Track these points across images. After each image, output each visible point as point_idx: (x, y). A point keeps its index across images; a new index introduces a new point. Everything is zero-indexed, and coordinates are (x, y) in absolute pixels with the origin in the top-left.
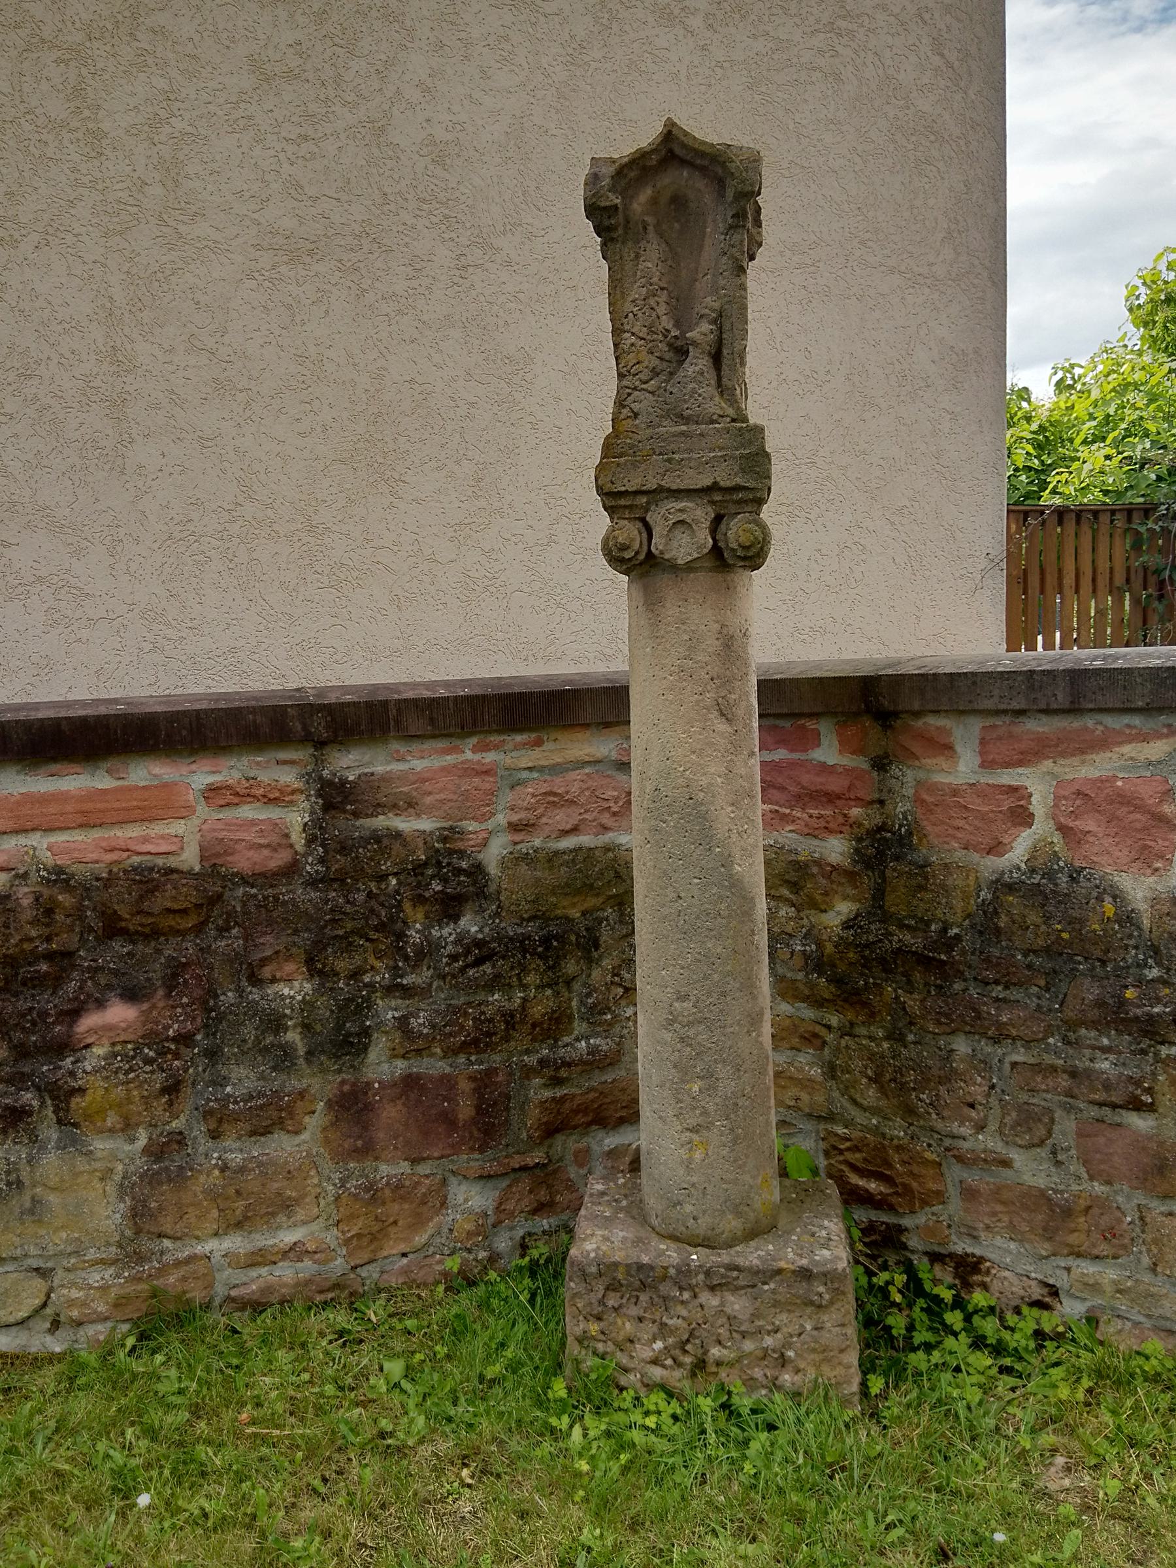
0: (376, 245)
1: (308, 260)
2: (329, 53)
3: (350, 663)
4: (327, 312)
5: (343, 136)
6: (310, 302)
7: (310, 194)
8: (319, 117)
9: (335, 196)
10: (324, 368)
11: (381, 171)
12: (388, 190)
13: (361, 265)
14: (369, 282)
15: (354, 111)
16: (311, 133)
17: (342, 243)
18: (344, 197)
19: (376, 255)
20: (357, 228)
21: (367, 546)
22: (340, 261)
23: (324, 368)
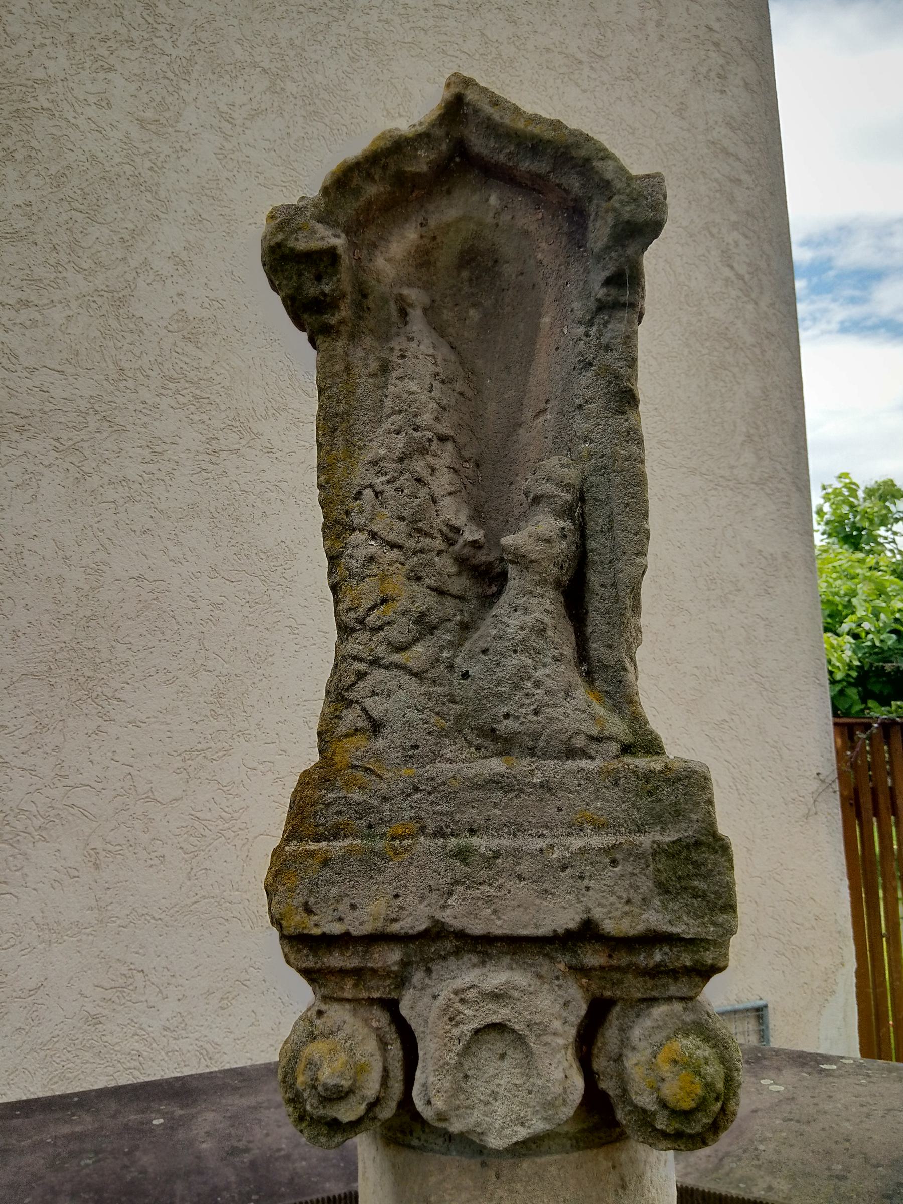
0: (106, 424)
1: (15, 436)
2: (65, 217)
3: (19, 947)
4: (34, 497)
5: (74, 304)
6: (13, 484)
7: (26, 364)
8: (46, 282)
9: (59, 368)
10: (24, 562)
11: (120, 344)
12: (126, 365)
13: (85, 445)
14: (94, 465)
15: (90, 279)
16: (34, 298)
17: (63, 420)
18: (70, 370)
19: (106, 435)
20: (83, 405)
21: (59, 784)
22: (57, 440)
23: (24, 562)
